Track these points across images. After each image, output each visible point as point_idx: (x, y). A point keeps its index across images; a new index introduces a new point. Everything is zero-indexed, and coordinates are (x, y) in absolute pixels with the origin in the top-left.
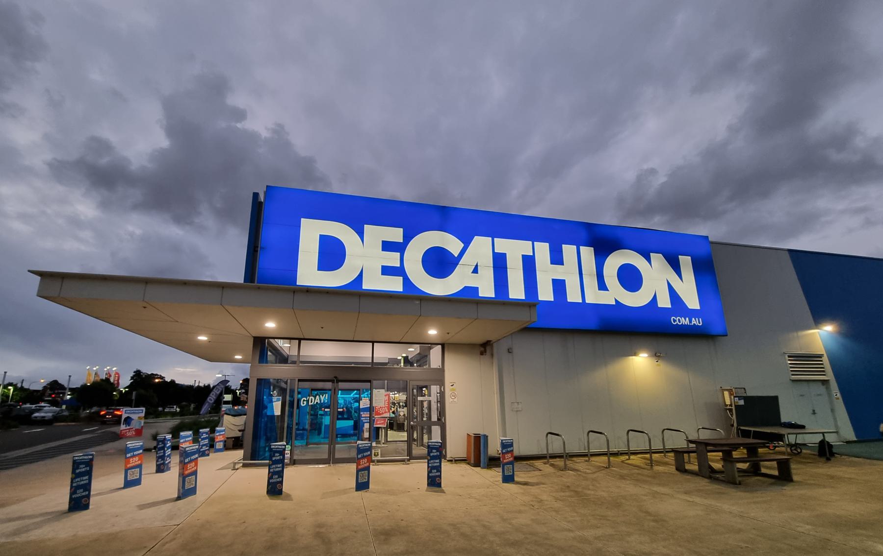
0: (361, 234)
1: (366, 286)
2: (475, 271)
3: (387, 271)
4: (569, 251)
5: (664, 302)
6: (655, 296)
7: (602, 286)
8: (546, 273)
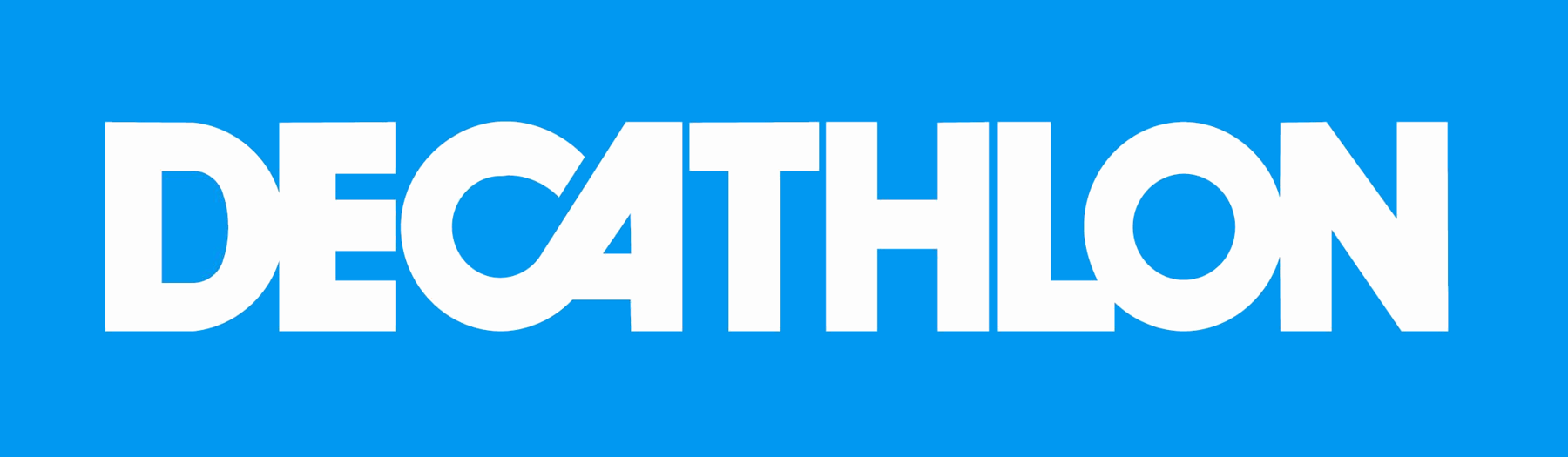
0: (270, 155)
1: (291, 320)
2: (621, 243)
3: (353, 266)
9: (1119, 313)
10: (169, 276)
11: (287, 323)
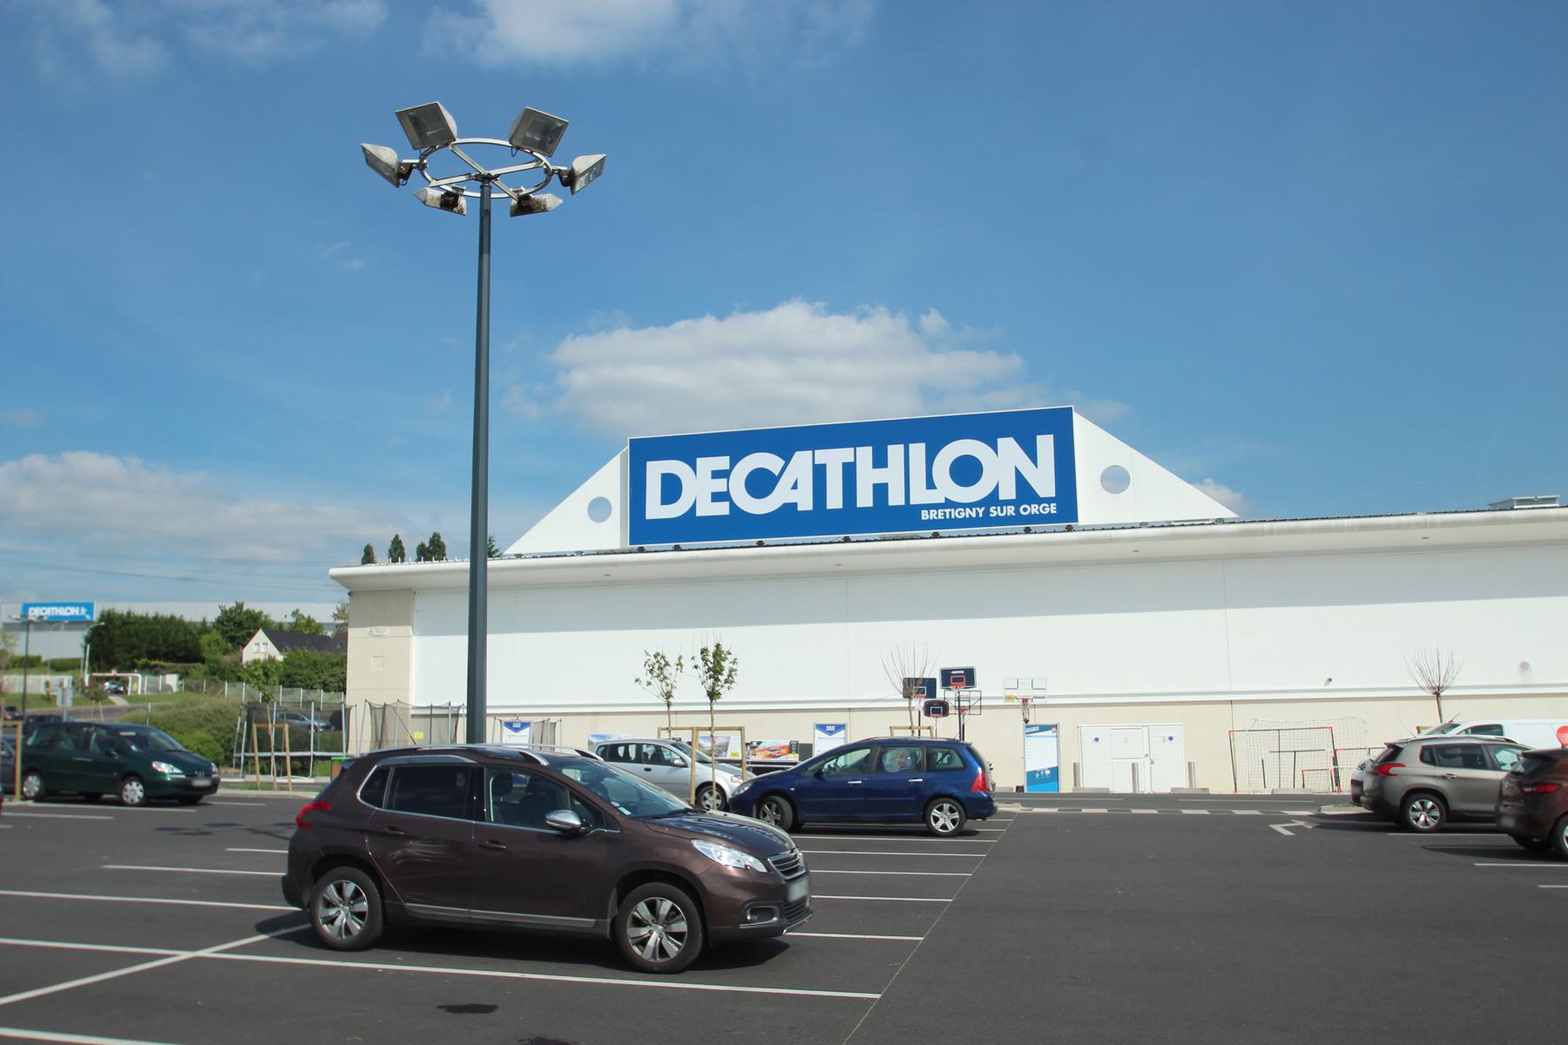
0: (694, 468)
1: (699, 513)
2: (795, 487)
3: (717, 497)
4: (895, 452)
5: (1008, 492)
6: (997, 487)
7: (930, 485)
8: (867, 478)
9: (946, 499)
10: (662, 504)
11: (698, 514)
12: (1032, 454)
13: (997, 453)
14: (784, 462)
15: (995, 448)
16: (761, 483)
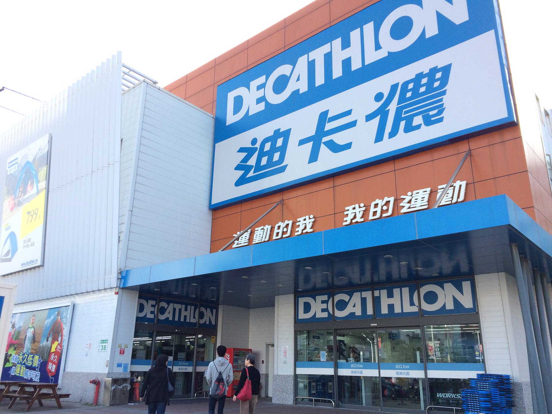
2: (354, 306)
3: (323, 310)
12: (461, 290)
13: (444, 290)
14: (349, 297)
15: (443, 288)
16: (342, 305)
